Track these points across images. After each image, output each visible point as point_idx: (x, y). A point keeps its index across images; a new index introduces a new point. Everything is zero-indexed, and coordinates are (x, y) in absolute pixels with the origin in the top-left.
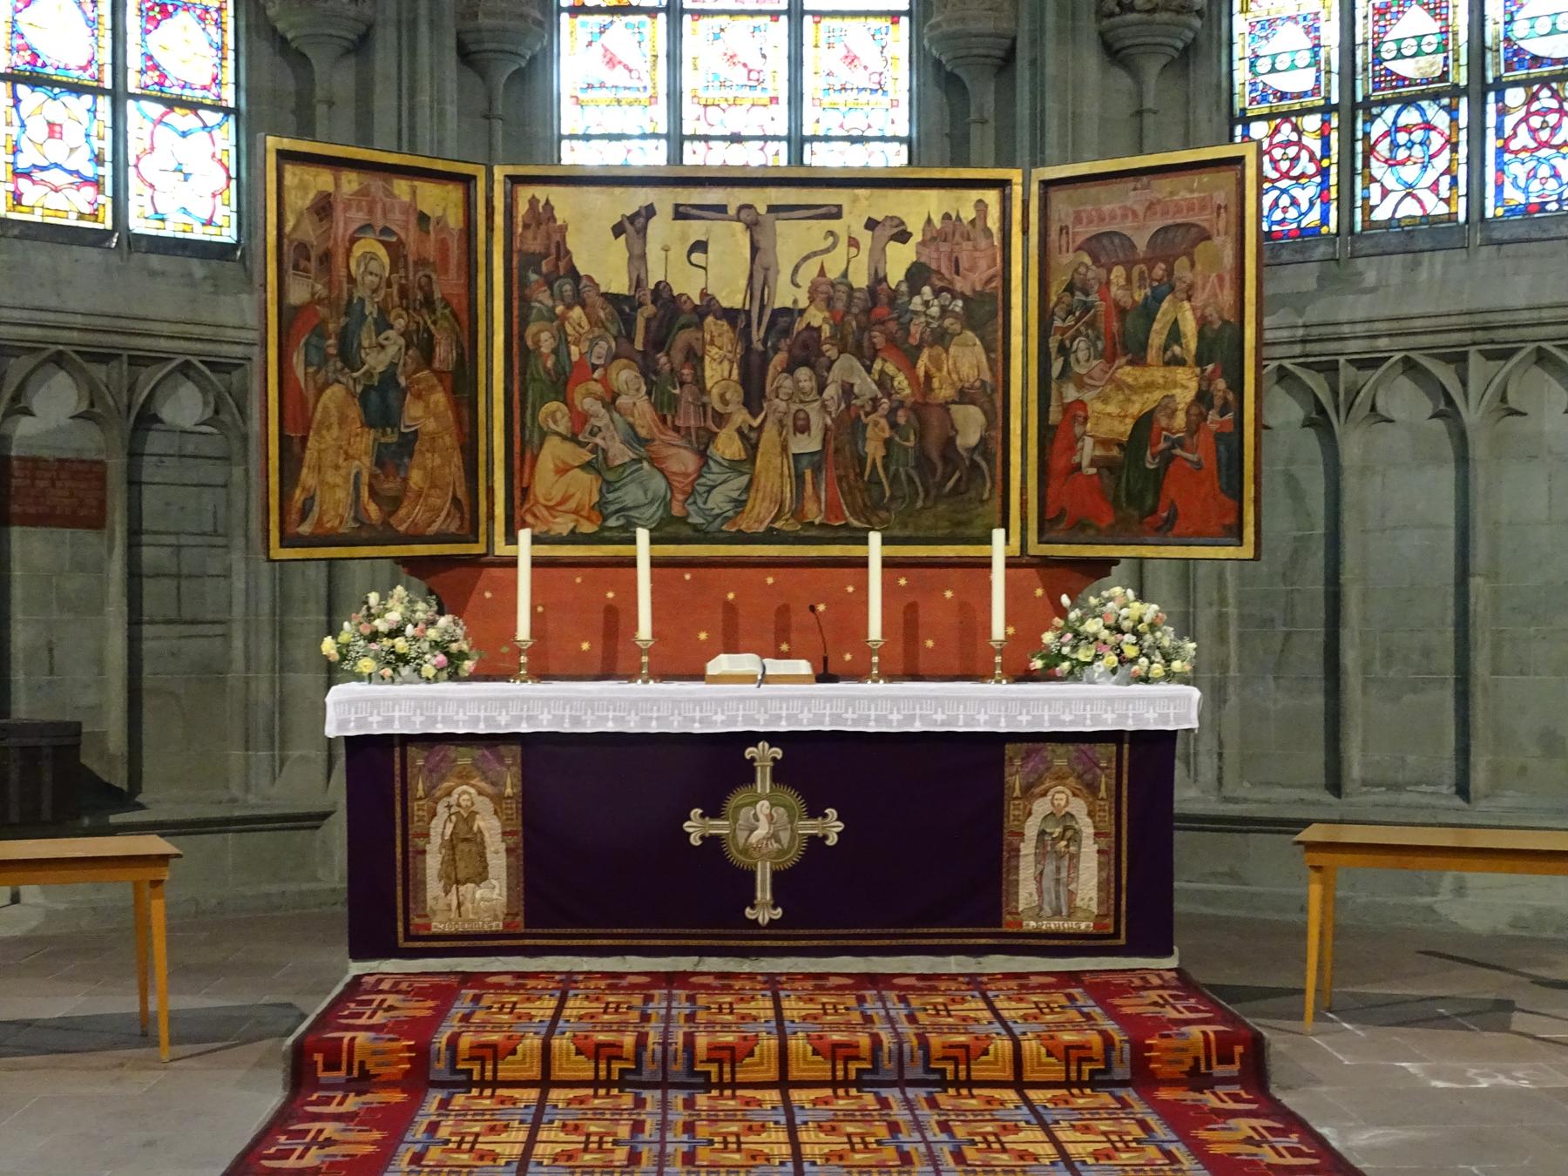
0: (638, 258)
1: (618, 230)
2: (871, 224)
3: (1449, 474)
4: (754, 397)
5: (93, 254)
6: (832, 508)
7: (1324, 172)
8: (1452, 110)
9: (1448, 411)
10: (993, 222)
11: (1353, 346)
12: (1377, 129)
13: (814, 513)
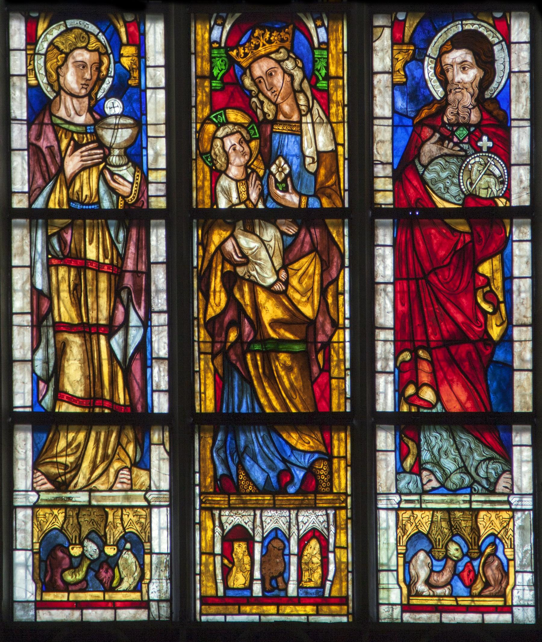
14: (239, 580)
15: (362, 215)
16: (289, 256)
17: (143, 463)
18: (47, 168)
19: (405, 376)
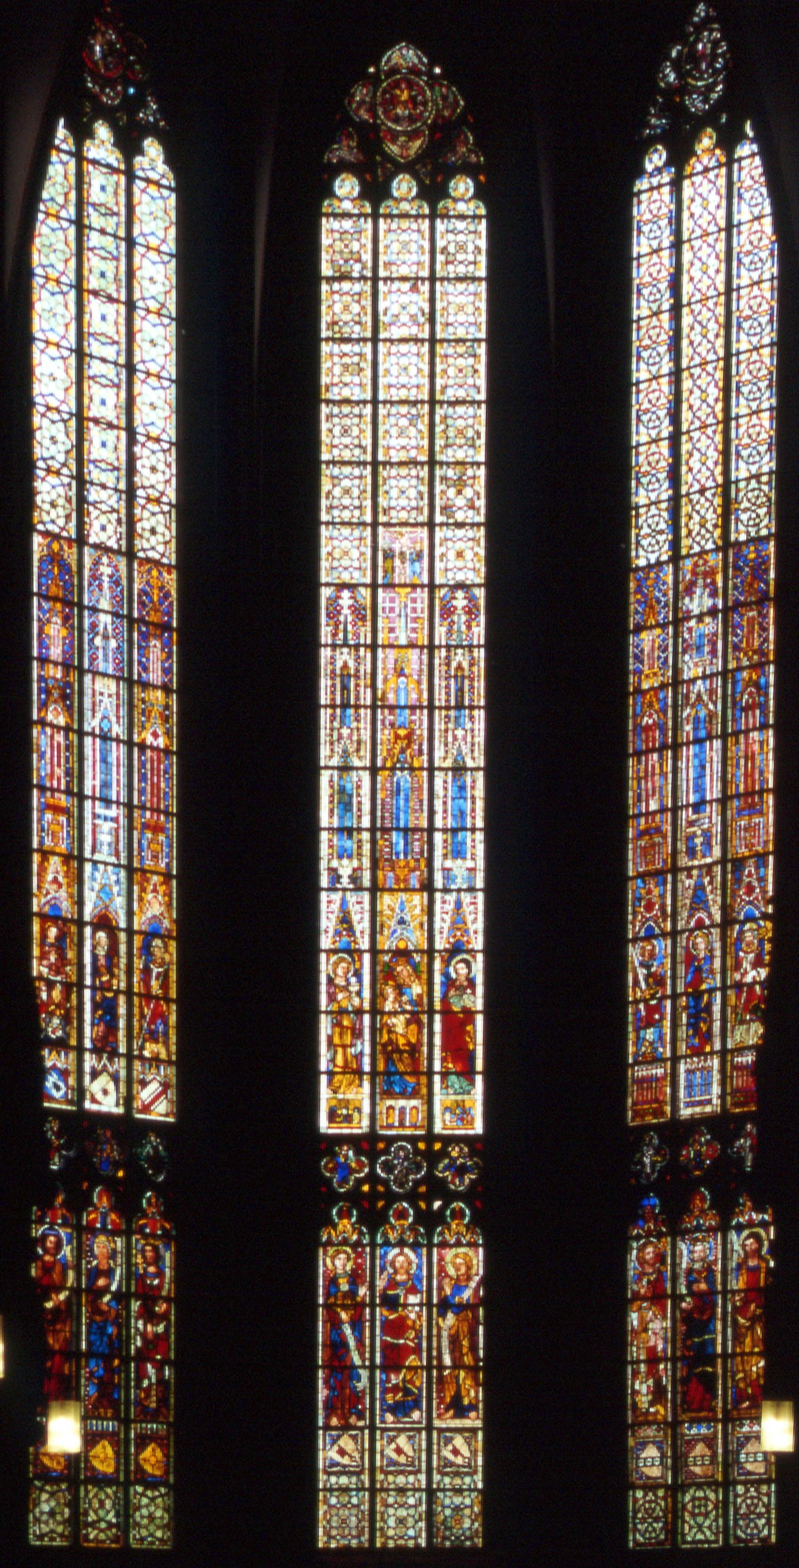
12: (688, 1498)
14: (390, 1121)
15: (431, 1012)
16: (408, 1023)
17: (360, 1085)
18: (332, 998)
19: (444, 1060)
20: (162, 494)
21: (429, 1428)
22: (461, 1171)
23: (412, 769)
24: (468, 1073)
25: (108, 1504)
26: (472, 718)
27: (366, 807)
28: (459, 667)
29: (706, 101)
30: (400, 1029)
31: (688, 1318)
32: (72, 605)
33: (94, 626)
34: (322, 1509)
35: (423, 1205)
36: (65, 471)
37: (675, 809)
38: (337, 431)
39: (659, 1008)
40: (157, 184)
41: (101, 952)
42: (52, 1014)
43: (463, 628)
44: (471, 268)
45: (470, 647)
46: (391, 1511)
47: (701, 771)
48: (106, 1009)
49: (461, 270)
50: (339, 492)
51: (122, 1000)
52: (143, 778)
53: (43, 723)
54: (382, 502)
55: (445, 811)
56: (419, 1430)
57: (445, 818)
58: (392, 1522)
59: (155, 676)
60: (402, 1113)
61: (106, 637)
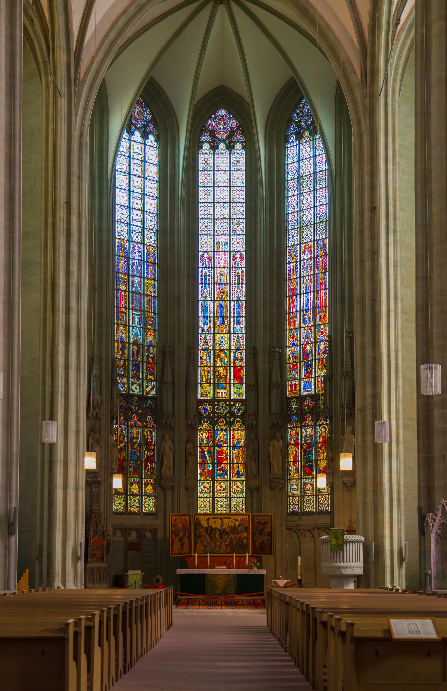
0: (208, 523)
1: (206, 520)
2: (234, 519)
3: (314, 544)
4: (221, 538)
5: (139, 516)
6: (230, 550)
7: (299, 504)
8: (313, 498)
9: (313, 536)
10: (248, 519)
11: (302, 527)
13: (228, 551)
14: (219, 396)
15: (230, 367)
16: (224, 370)
18: (202, 363)
19: (234, 380)
20: (154, 227)
21: (230, 480)
22: (239, 410)
23: (225, 301)
24: (241, 383)
25: (137, 501)
26: (242, 287)
27: (212, 311)
28: (238, 273)
29: (306, 124)
30: (221, 371)
31: (305, 451)
32: (127, 258)
33: (133, 263)
34: (199, 502)
35: (228, 419)
36: (126, 222)
37: (301, 311)
38: (203, 211)
39: (296, 365)
40: (153, 147)
41: (135, 351)
42: (120, 368)
43: (239, 263)
44: (241, 167)
45: (241, 267)
46: (219, 503)
47: (307, 300)
48: (136, 367)
49: (238, 168)
50: (204, 226)
51: (141, 363)
52: (147, 304)
53: (118, 289)
54: (216, 229)
55: (234, 312)
56: (227, 481)
57: (234, 314)
58: (219, 506)
59: (151, 276)
60: (222, 394)
61: (137, 266)
